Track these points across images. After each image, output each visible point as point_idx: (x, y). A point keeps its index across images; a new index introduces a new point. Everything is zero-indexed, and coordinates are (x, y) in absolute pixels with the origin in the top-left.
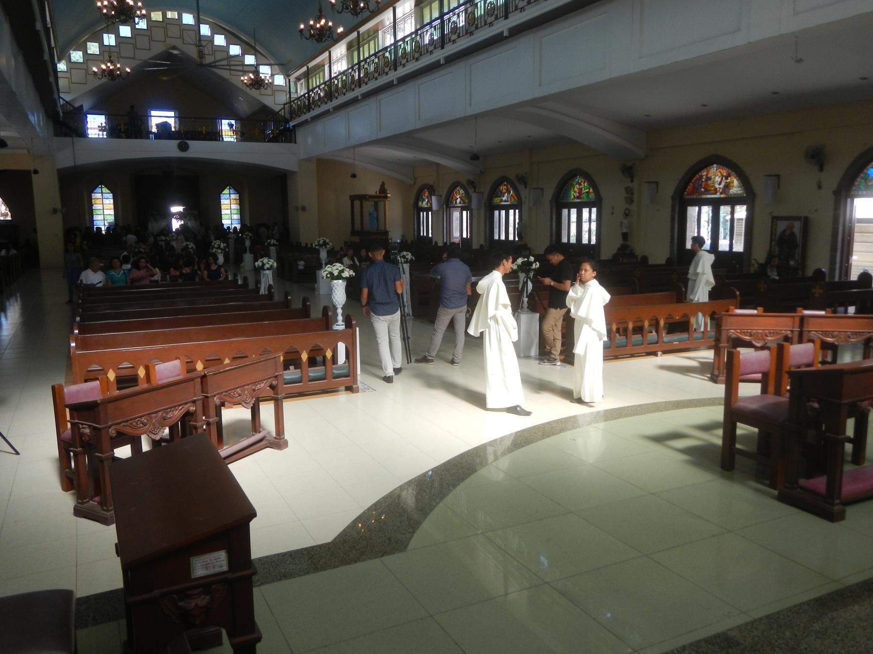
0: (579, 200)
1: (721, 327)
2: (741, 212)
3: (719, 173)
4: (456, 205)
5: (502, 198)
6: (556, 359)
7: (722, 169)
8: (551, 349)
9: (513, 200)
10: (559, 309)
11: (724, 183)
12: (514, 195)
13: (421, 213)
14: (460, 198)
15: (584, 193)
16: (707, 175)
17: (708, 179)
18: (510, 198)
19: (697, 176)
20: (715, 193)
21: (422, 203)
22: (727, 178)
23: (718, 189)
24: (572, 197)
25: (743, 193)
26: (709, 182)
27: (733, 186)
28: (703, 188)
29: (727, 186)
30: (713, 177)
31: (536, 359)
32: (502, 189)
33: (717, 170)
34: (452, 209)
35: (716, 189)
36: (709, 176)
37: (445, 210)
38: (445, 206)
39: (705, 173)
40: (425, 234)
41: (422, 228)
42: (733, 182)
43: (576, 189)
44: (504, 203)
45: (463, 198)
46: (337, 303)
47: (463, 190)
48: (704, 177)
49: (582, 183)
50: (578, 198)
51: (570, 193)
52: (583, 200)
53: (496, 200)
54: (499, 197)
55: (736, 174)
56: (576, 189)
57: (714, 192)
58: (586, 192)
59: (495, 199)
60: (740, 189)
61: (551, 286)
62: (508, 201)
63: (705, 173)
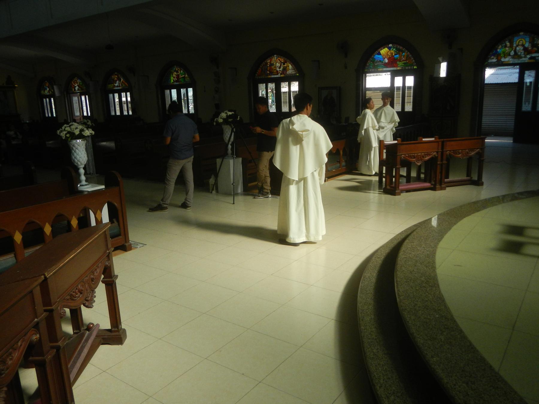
0: (177, 83)
1: (397, 153)
2: (295, 87)
3: (278, 61)
4: (75, 92)
5: (115, 84)
6: (268, 193)
7: (280, 58)
8: (262, 185)
9: (124, 85)
10: (270, 152)
11: (282, 67)
12: (124, 81)
13: (44, 100)
14: (78, 86)
15: (181, 78)
16: (270, 62)
17: (272, 65)
18: (122, 84)
19: (264, 63)
20: (277, 74)
21: (44, 91)
22: (284, 64)
23: (279, 71)
24: (172, 81)
25: (296, 74)
26: (273, 67)
27: (289, 69)
28: (268, 71)
29: (285, 69)
30: (274, 63)
31: (242, 195)
32: (114, 78)
33: (277, 59)
34: (71, 95)
35: (277, 71)
36: (272, 62)
37: (66, 95)
38: (65, 93)
40: (50, 115)
41: (46, 111)
42: (289, 67)
43: (174, 75)
44: (116, 88)
46: (79, 163)
47: (80, 80)
48: (269, 64)
49: (179, 71)
50: (177, 81)
51: (170, 79)
52: (181, 83)
53: (110, 86)
54: (113, 84)
55: (290, 61)
56: (174, 75)
57: (276, 73)
58: (183, 77)
60: (294, 71)
61: (260, 134)
62: (119, 86)
63: (269, 61)
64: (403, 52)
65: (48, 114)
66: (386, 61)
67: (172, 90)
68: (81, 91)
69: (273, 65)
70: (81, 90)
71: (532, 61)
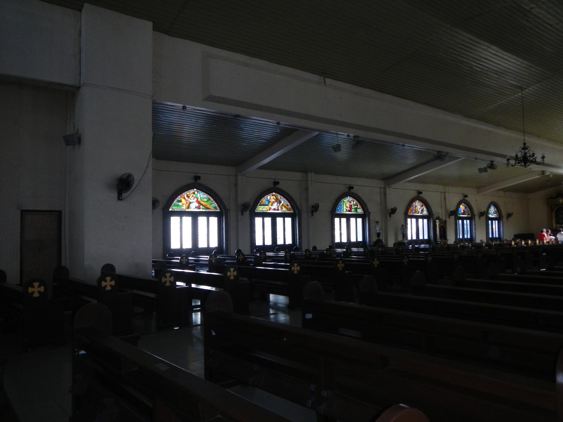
5: (270, 207)
9: (284, 209)
20: (419, 213)
26: (416, 208)
29: (422, 211)
32: (270, 198)
36: (416, 205)
39: (414, 204)
44: (271, 211)
45: (203, 203)
49: (352, 202)
50: (349, 211)
52: (353, 213)
54: (267, 205)
59: (259, 207)
62: (278, 210)
65: (175, 245)
66: (462, 212)
68: (204, 210)
70: (202, 209)
71: (495, 217)
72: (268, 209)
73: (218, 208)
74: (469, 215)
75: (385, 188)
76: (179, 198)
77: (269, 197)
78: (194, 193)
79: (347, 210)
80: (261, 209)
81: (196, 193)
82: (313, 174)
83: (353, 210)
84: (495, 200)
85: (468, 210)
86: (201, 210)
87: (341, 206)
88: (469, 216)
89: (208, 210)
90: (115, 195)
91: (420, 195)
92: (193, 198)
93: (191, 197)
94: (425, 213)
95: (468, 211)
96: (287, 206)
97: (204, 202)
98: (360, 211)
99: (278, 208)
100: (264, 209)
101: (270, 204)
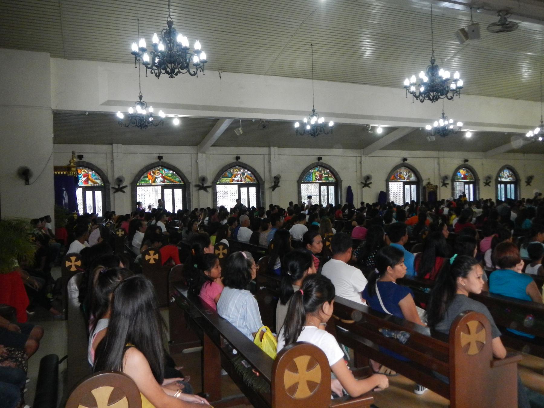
4: (153, 184)
5: (233, 178)
14: (162, 177)
15: (324, 177)
20: (404, 179)
22: (409, 173)
24: (314, 179)
26: (402, 174)
29: (409, 177)
36: (401, 171)
39: (399, 170)
42: (411, 175)
45: (167, 177)
49: (322, 171)
50: (319, 180)
52: (323, 181)
58: (326, 177)
59: (223, 179)
62: (241, 181)
64: (469, 172)
66: (463, 176)
67: (96, 192)
68: (169, 184)
69: (401, 173)
70: (167, 182)
72: (231, 180)
73: (182, 181)
74: (472, 179)
75: (361, 156)
76: (145, 175)
77: (232, 171)
78: (159, 170)
79: (316, 179)
80: (224, 181)
81: (161, 170)
82: (276, 148)
83: (323, 178)
84: (511, 163)
85: (471, 174)
86: (166, 184)
87: (311, 176)
88: (472, 180)
89: (172, 184)
90: (23, 182)
91: (406, 162)
92: (158, 174)
93: (156, 173)
94: (413, 178)
95: (471, 176)
96: (251, 178)
97: (169, 177)
98: (331, 179)
99: (242, 179)
100: (227, 181)
101: (233, 176)
